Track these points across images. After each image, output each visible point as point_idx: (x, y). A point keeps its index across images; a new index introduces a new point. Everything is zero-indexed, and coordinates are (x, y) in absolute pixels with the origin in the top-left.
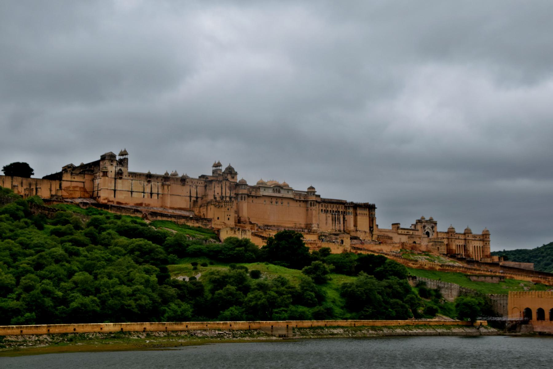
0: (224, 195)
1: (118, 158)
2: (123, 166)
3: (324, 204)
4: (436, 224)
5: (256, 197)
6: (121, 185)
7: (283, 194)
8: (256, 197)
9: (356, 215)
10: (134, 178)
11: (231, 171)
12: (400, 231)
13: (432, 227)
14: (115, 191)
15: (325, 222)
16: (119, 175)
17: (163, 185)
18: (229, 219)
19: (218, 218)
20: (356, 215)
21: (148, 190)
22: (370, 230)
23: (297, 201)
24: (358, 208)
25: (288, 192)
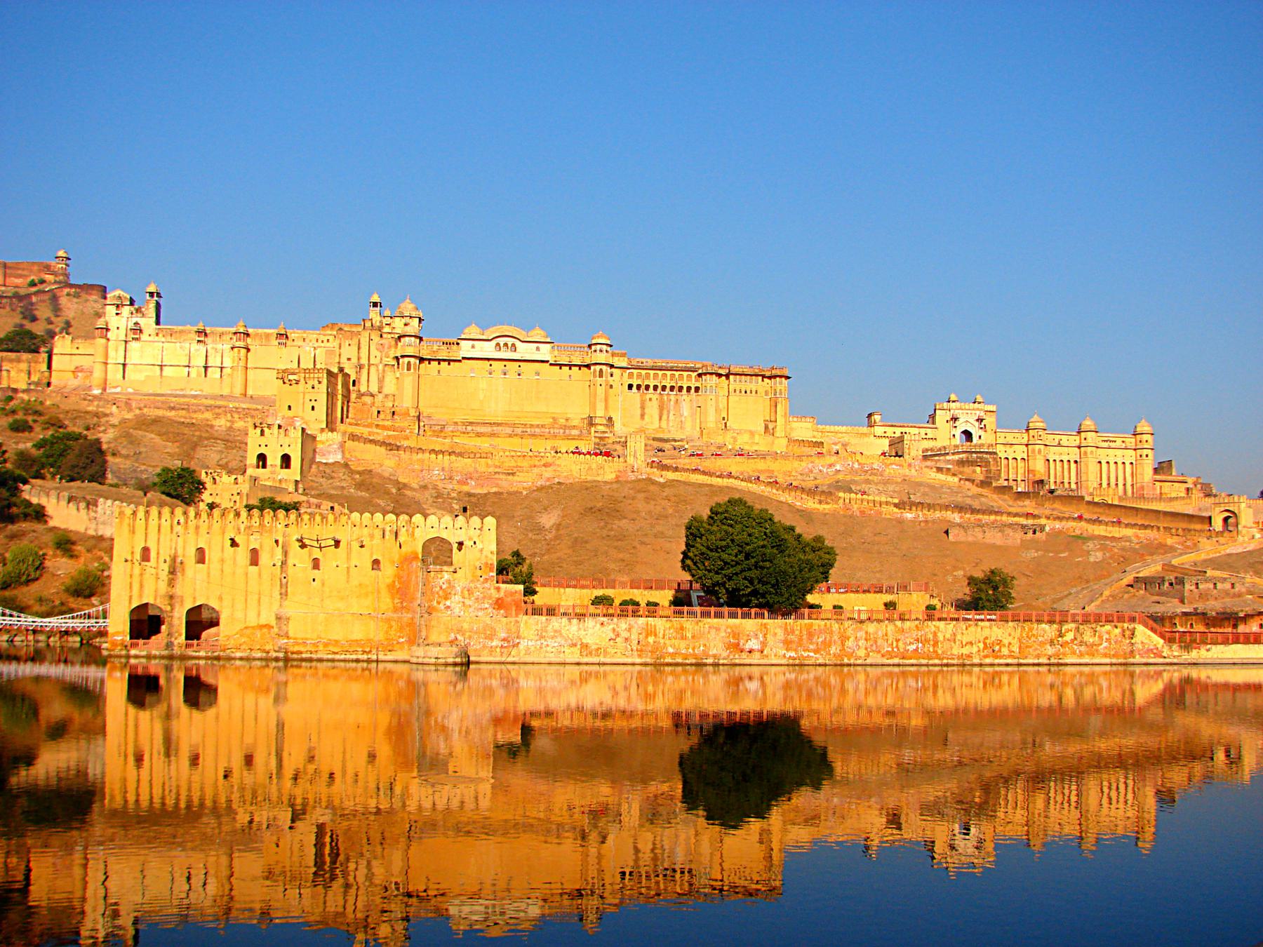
0: (364, 361)
2: (144, 316)
3: (635, 372)
5: (449, 361)
7: (525, 351)
8: (449, 361)
10: (169, 339)
13: (980, 420)
14: (124, 365)
15: (639, 412)
18: (313, 408)
19: (290, 407)
22: (766, 427)
23: (561, 366)
24: (731, 377)
25: (538, 349)
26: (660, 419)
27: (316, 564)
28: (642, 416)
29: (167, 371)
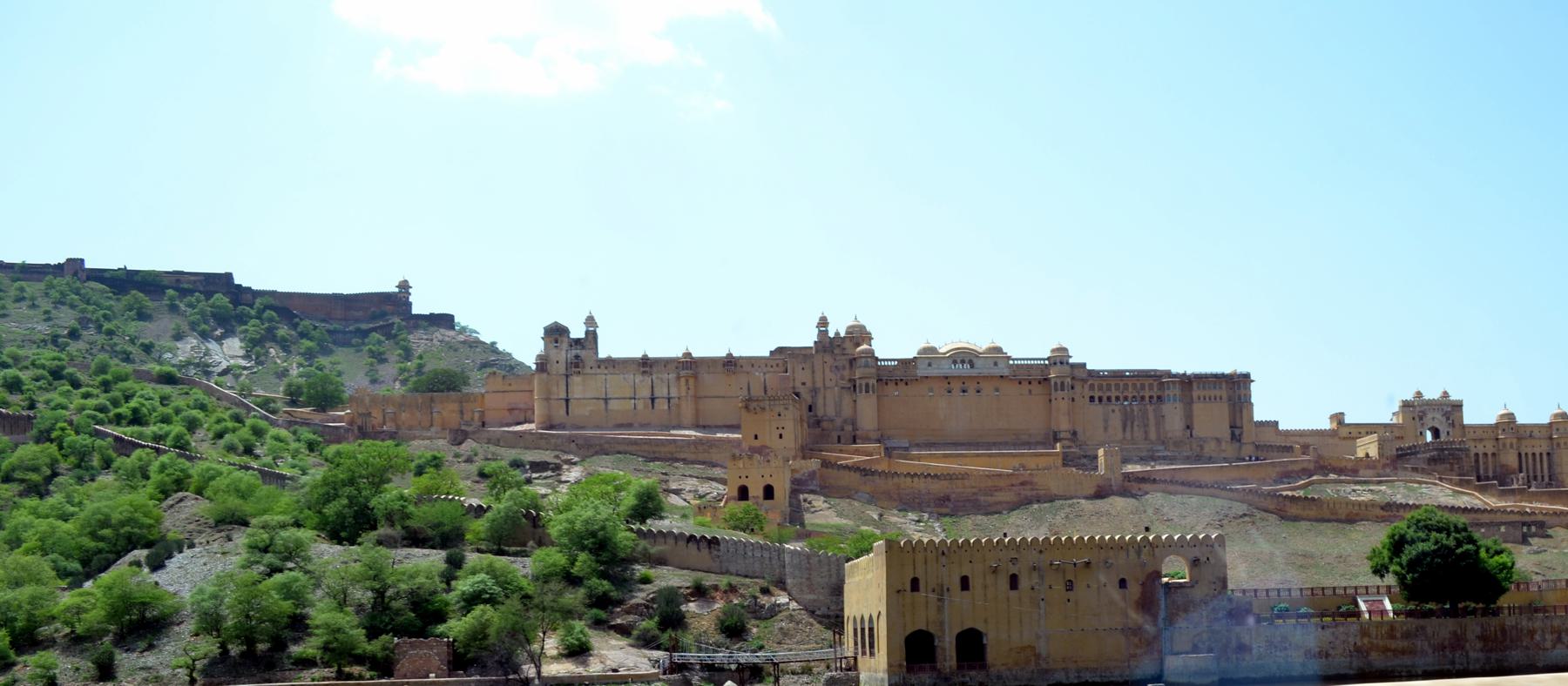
0: (819, 384)
1: (578, 332)
2: (583, 348)
4: (1458, 406)
6: (578, 387)
7: (982, 368)
9: (1188, 403)
11: (859, 335)
12: (1344, 432)
13: (1447, 415)
16: (576, 365)
17: (678, 378)
20: (1188, 403)
21: (646, 393)
22: (1233, 434)
24: (1195, 385)
26: (1124, 430)
27: (1070, 586)
28: (1106, 429)
29: (613, 405)
